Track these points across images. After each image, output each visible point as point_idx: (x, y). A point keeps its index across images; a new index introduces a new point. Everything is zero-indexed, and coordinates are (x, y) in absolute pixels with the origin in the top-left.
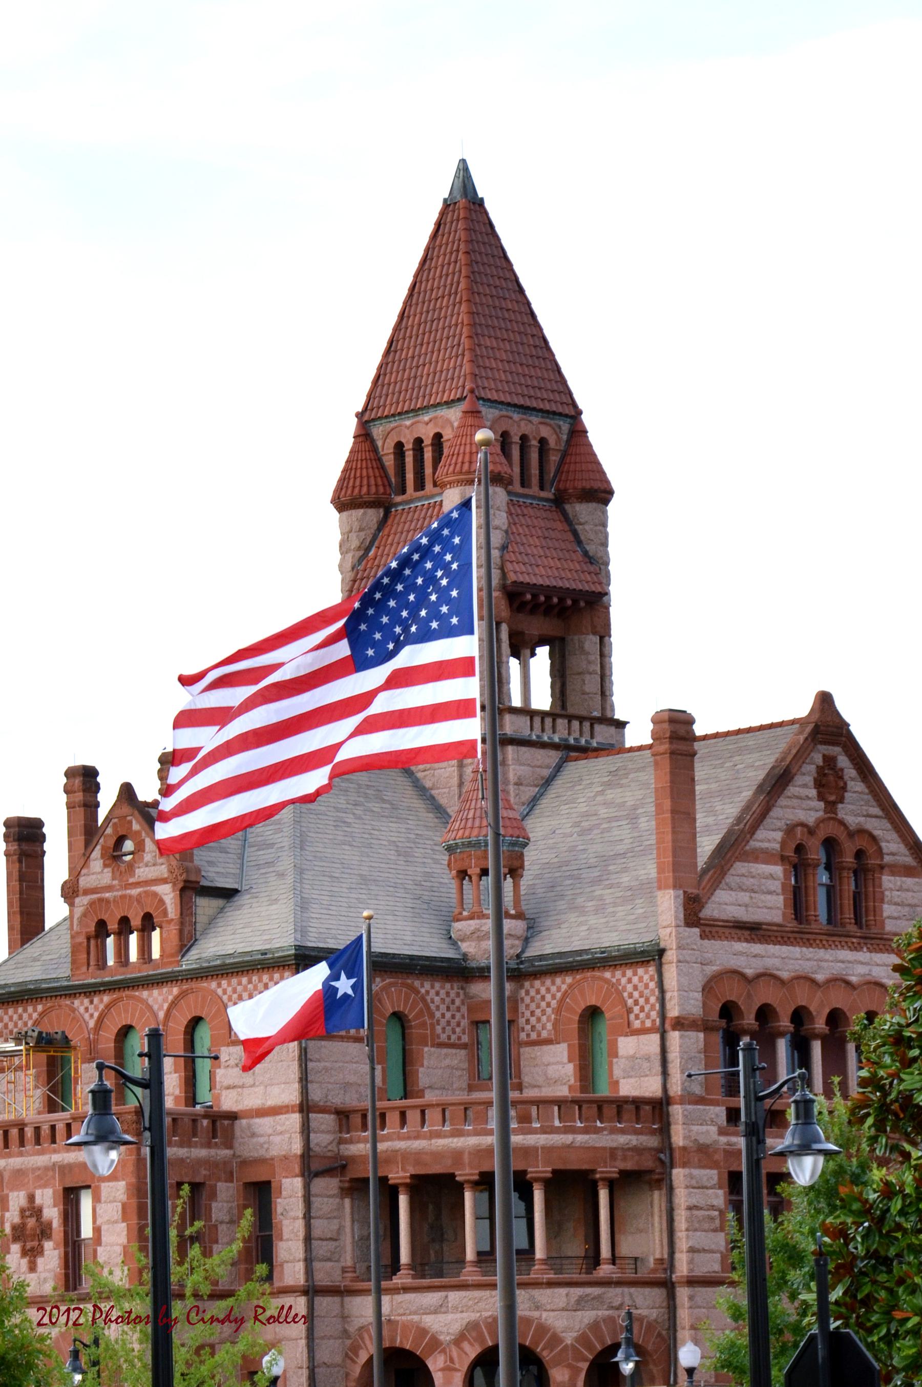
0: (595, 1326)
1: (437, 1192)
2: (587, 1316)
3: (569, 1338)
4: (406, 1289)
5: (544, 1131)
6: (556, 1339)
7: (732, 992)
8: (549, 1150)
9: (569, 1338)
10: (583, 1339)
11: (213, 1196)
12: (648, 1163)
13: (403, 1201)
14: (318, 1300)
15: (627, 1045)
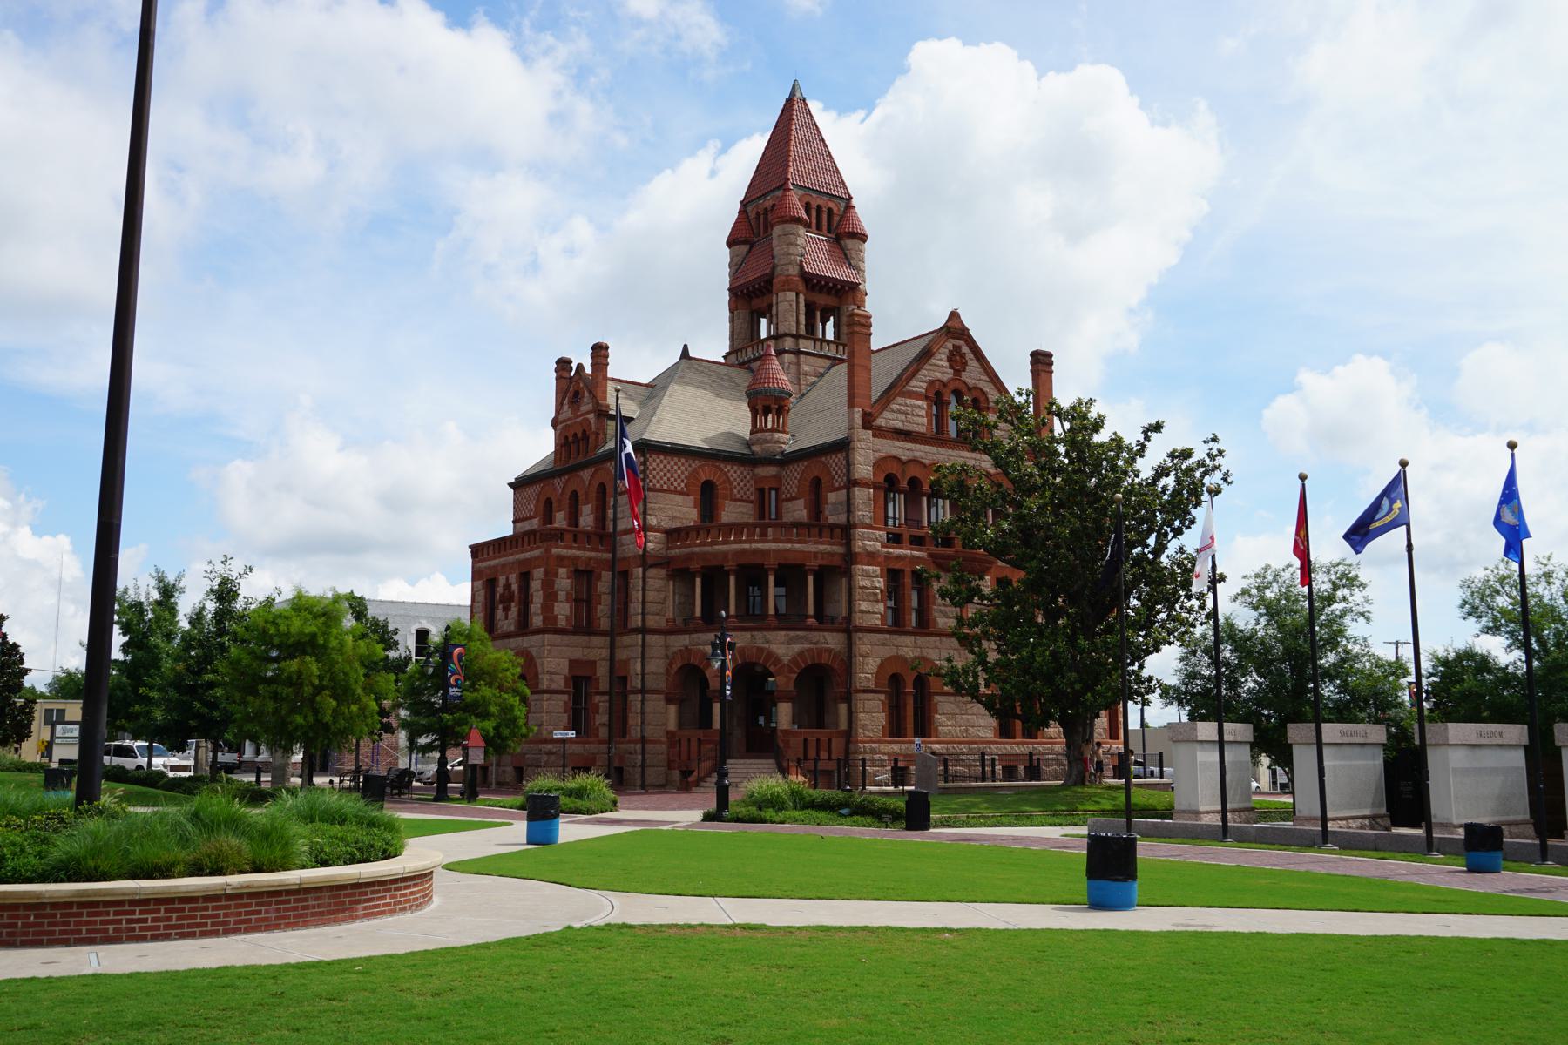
0: (801, 654)
1: (713, 577)
2: (797, 648)
3: (786, 660)
4: (697, 631)
5: (774, 541)
6: (778, 660)
7: (894, 469)
8: (777, 552)
9: (786, 660)
10: (794, 661)
11: (599, 578)
12: (837, 561)
13: (698, 581)
14: (648, 637)
15: (832, 497)
